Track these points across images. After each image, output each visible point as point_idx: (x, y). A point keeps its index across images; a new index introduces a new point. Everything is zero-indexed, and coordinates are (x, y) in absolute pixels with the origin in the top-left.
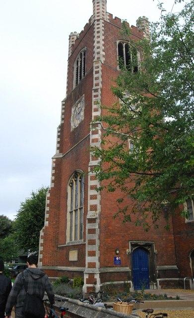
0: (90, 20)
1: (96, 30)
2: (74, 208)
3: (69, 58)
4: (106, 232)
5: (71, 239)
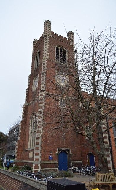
0: (42, 35)
1: (45, 41)
2: (32, 131)
3: (33, 53)
4: (45, 142)
5: (30, 147)
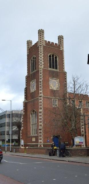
2: (33, 123)
4: (45, 132)
